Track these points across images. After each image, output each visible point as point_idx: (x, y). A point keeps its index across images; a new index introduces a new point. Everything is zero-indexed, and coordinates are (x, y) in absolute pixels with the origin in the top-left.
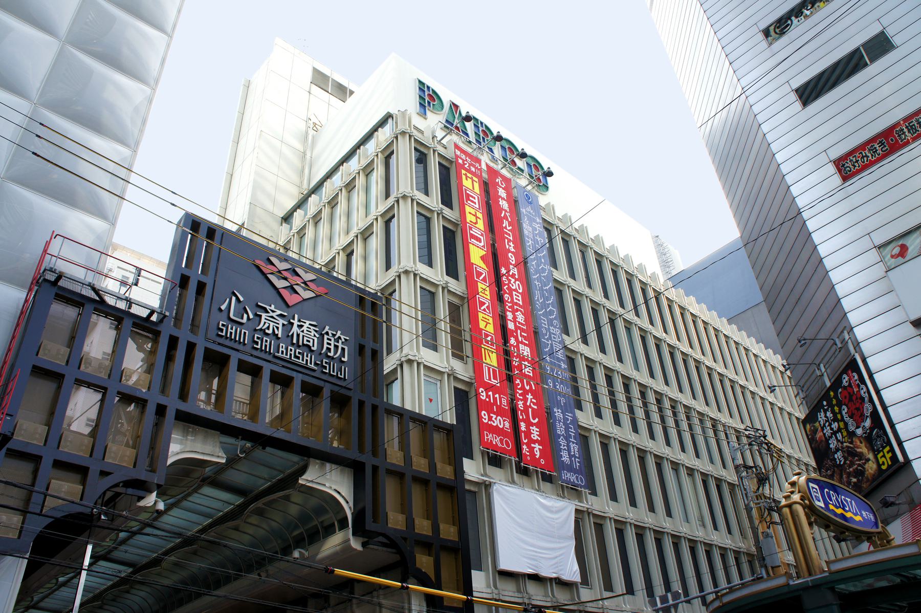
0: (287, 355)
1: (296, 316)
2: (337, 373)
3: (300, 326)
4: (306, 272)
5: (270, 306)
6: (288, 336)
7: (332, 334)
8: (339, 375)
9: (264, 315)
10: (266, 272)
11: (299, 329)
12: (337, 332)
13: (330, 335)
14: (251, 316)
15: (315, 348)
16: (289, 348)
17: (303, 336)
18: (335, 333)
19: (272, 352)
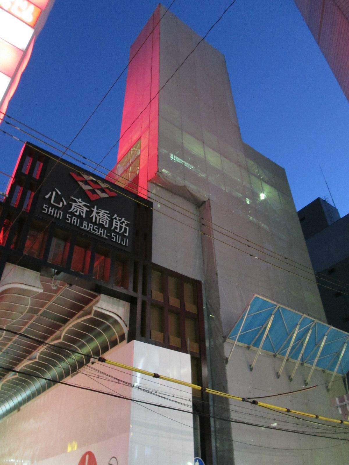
0: (88, 228)
1: (96, 207)
2: (121, 242)
3: (98, 213)
4: (103, 183)
5: (79, 199)
6: (90, 218)
7: (119, 219)
9: (74, 204)
10: (77, 180)
12: (122, 219)
13: (118, 219)
14: (65, 203)
15: (107, 226)
16: (90, 224)
17: (99, 219)
18: (120, 219)
19: (78, 225)
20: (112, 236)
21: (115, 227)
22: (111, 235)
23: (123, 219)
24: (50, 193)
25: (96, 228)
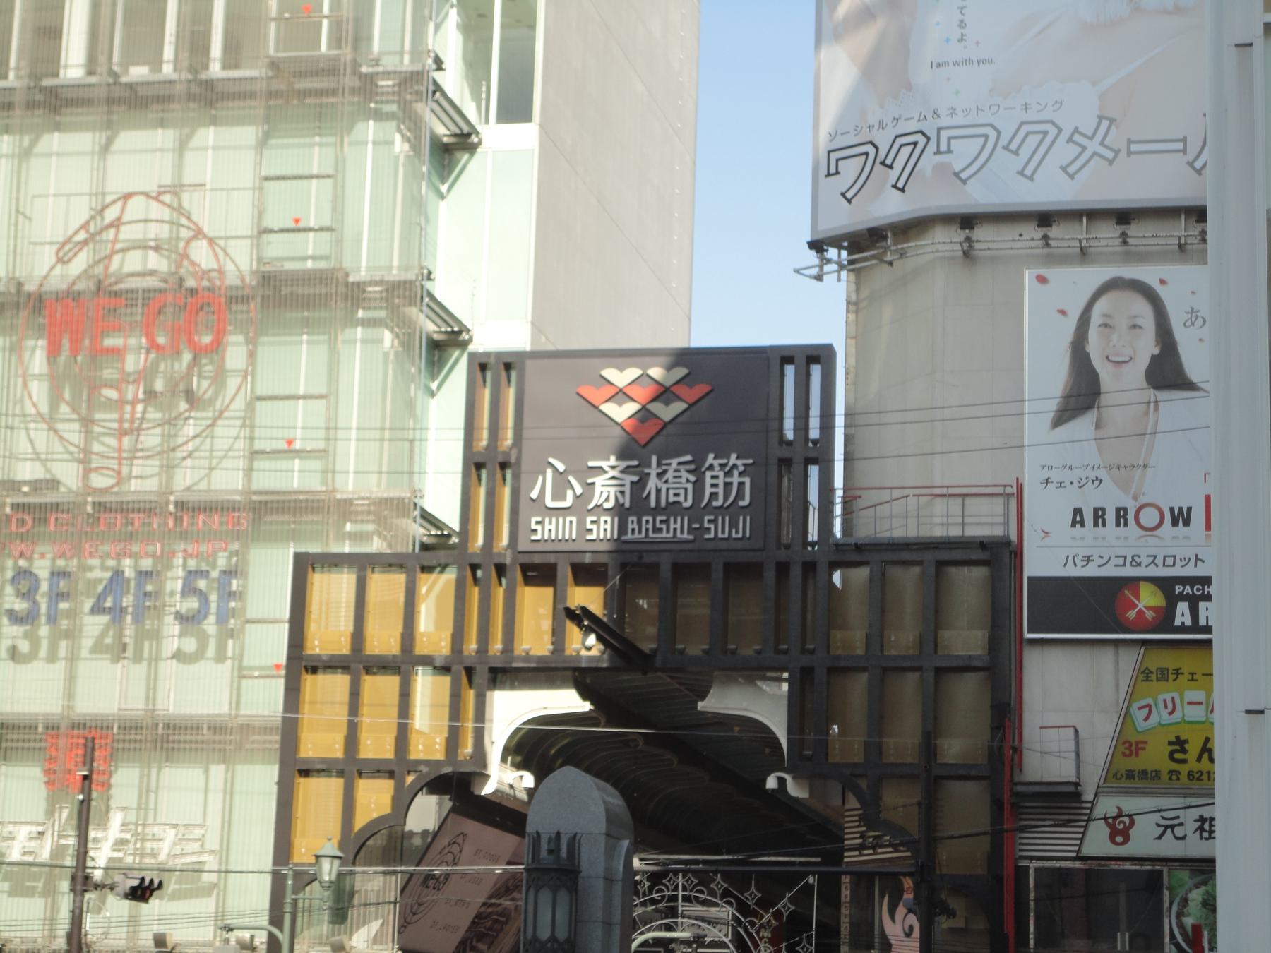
0: (640, 532)
3: (659, 475)
5: (608, 459)
8: (734, 535)
12: (728, 458)
13: (717, 468)
17: (668, 489)
18: (724, 461)
20: (706, 525)
21: (712, 494)
22: (702, 523)
23: (733, 459)
24: (540, 478)
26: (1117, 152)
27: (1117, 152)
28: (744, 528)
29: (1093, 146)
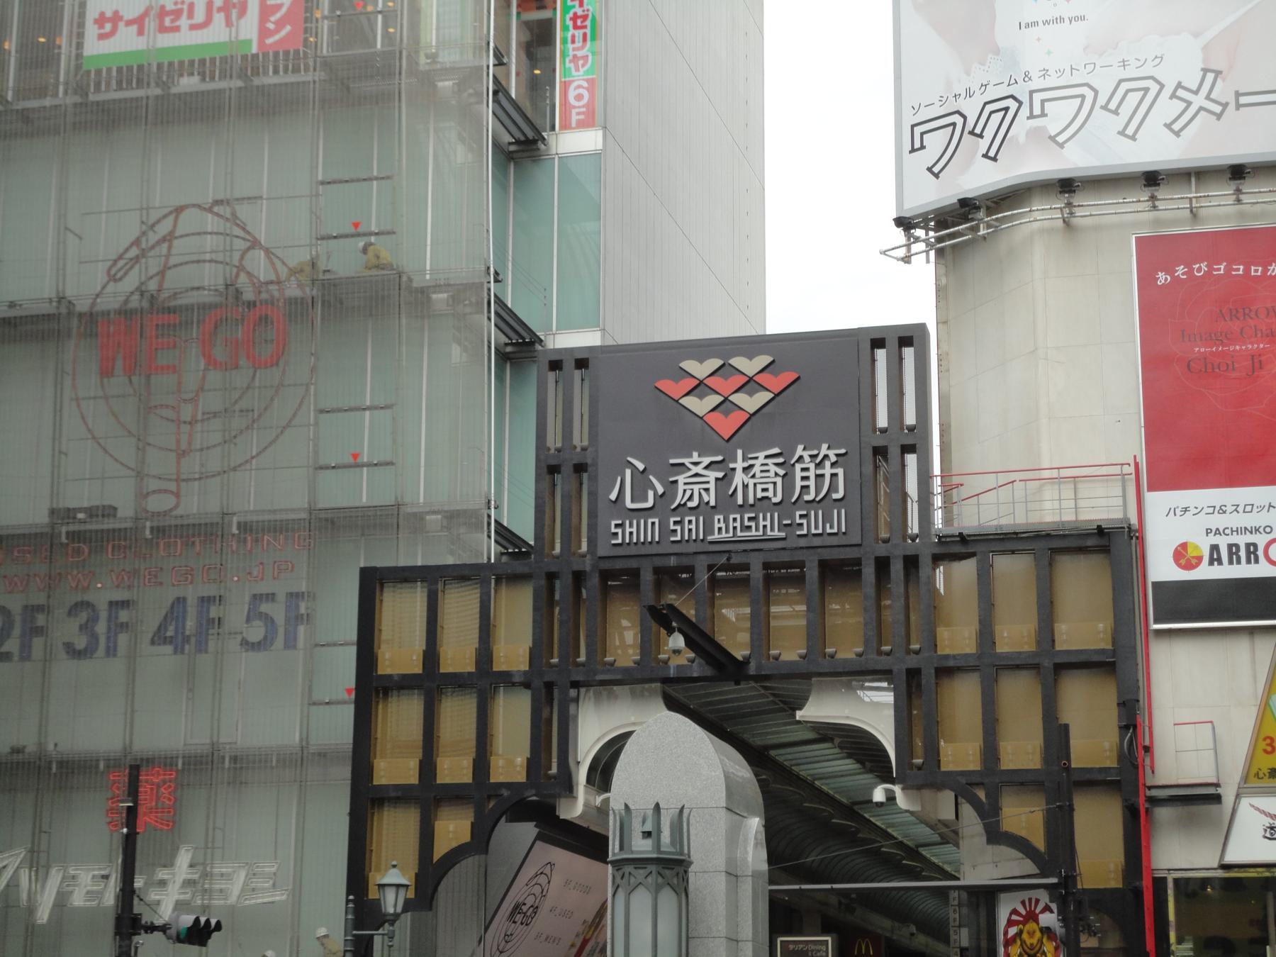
0: (727, 531)
1: (740, 452)
7: (811, 456)
8: (829, 531)
9: (681, 479)
10: (676, 399)
11: (747, 475)
12: (819, 449)
13: (807, 459)
18: (815, 452)
21: (802, 487)
22: (793, 518)
23: (824, 450)
25: (750, 519)
26: (1225, 106)
27: (1225, 106)
28: (838, 522)
29: (1199, 100)
